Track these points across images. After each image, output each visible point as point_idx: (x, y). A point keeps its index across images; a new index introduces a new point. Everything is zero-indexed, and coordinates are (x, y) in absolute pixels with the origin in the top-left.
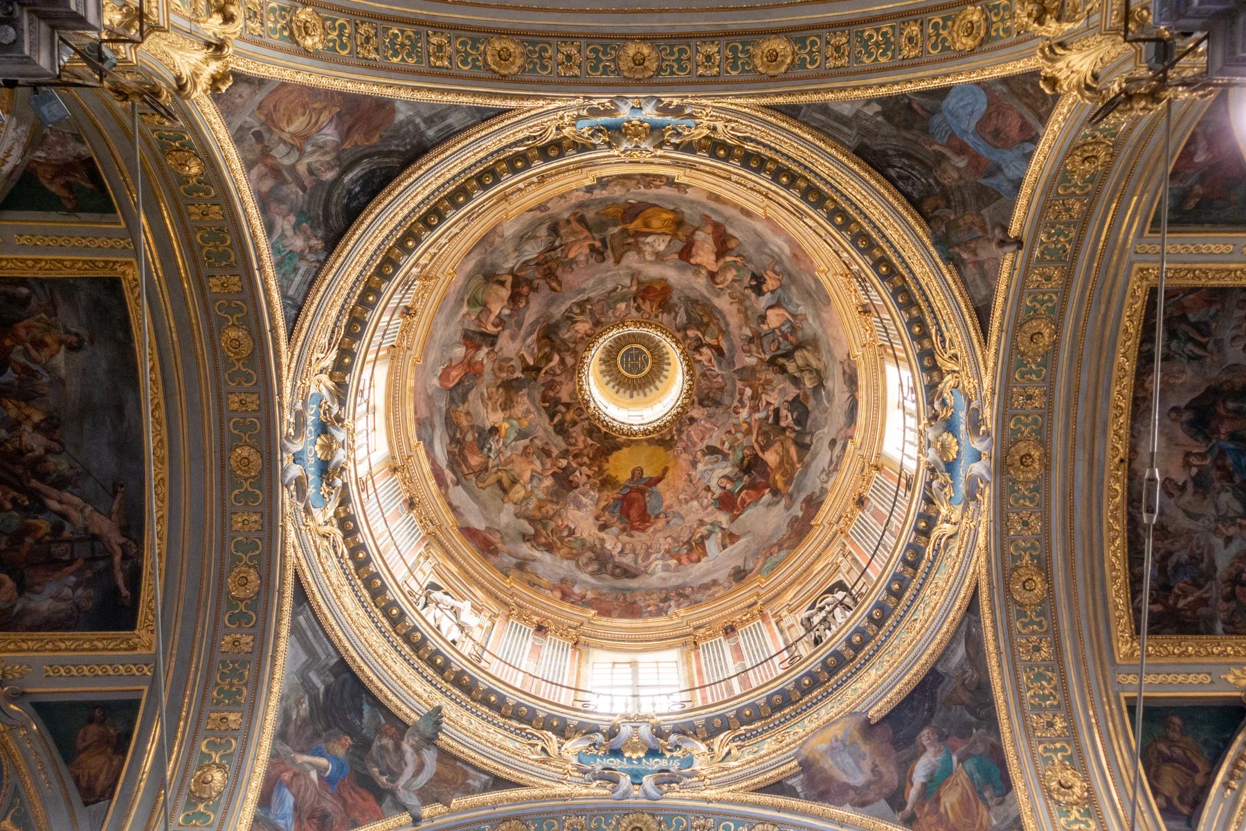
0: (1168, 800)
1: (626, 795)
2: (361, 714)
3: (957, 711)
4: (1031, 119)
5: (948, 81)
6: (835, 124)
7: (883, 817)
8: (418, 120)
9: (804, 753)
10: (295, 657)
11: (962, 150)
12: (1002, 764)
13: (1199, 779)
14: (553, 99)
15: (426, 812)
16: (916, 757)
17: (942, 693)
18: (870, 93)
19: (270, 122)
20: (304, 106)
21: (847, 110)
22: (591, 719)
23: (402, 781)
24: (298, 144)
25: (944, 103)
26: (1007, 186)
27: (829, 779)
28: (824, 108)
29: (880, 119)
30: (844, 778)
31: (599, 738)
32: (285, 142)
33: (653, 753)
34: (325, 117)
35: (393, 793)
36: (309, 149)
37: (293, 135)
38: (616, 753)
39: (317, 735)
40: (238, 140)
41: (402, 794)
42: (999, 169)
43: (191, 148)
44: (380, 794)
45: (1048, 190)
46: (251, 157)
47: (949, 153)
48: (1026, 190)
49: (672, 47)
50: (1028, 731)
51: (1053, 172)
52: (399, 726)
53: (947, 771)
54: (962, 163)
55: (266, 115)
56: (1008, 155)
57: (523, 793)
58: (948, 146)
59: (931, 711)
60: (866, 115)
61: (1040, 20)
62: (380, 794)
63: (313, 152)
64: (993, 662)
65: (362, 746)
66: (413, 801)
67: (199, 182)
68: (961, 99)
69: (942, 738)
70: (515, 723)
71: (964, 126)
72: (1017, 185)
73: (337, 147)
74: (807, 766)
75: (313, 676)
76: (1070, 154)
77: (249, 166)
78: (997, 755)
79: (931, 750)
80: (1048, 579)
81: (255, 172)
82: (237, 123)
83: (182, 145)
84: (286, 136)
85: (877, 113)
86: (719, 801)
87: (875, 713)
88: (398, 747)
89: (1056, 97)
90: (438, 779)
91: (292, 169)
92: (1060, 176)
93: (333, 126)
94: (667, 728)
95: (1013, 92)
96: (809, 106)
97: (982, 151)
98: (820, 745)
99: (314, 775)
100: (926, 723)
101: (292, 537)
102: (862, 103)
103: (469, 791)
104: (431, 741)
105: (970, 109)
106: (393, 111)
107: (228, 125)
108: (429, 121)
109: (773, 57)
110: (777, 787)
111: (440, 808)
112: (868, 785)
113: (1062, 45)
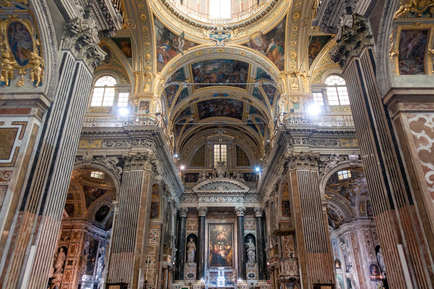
0: (311, 55)
1: (218, 46)
2: (170, 36)
3: (278, 36)
7: (262, 54)
9: (251, 38)
10: (156, 29)
12: (284, 49)
13: (318, 50)
15: (184, 52)
16: (270, 43)
17: (277, 32)
22: (212, 26)
23: (179, 47)
27: (255, 44)
30: (257, 45)
31: (213, 30)
33: (223, 33)
35: (178, 49)
38: (217, 33)
39: (163, 42)
41: (180, 49)
44: (176, 50)
50: (290, 44)
52: (176, 36)
53: (275, 47)
57: (201, 46)
59: (274, 35)
62: (176, 50)
64: (286, 30)
65: (171, 42)
66: (181, 50)
69: (275, 40)
70: (197, 28)
74: (251, 41)
75: (160, 31)
78: (283, 47)
79: (273, 42)
80: (300, 15)
86: (235, 47)
87: (264, 33)
88: (177, 41)
90: (185, 45)
94: (226, 28)
98: (253, 37)
99: (164, 50)
100: (273, 37)
101: (151, 7)
103: (191, 47)
104: (183, 38)
110: (245, 45)
111: (186, 51)
112: (261, 47)
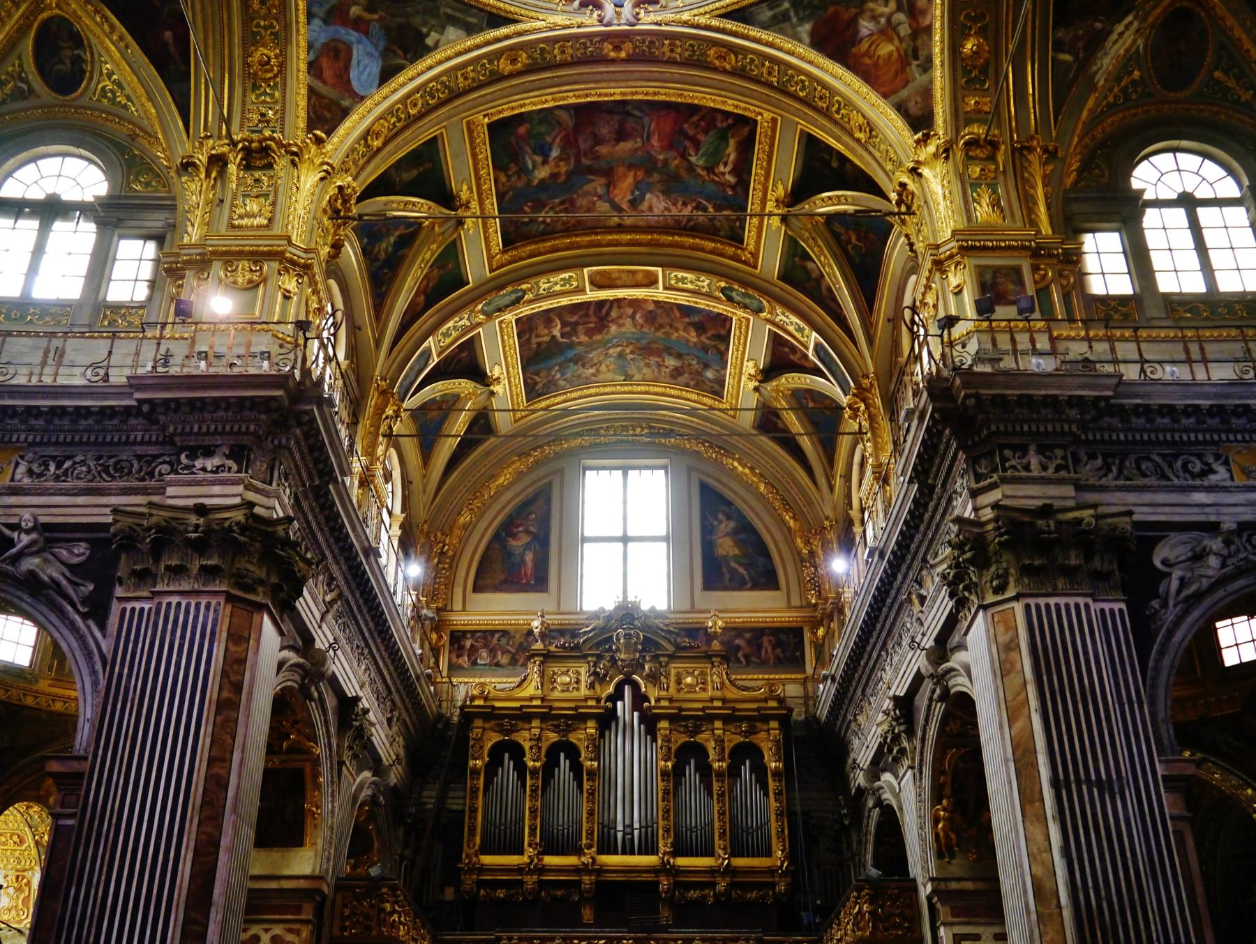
4: (318, 85)
5: (385, 90)
6: (458, 15)
8: (794, 20)
11: (358, 25)
14: (685, 24)
18: (438, 55)
19: (904, 62)
20: (876, 65)
21: (452, 32)
24: (889, 30)
25: (380, 63)
26: (315, 9)
28: (470, 30)
29: (425, 30)
32: (898, 36)
34: (864, 46)
36: (883, 20)
37: (891, 41)
40: (929, 60)
42: (326, 21)
43: (964, 68)
45: (287, 26)
46: (926, 37)
47: (367, 16)
48: (302, 18)
49: (592, 55)
51: (289, 48)
54: (355, 10)
55: (905, 71)
56: (323, 39)
58: (368, 22)
60: (436, 31)
61: (340, 188)
63: (881, 15)
67: (970, 28)
68: (369, 74)
71: (361, 47)
72: (310, 16)
73: (861, 13)
76: (282, 66)
77: (929, 30)
81: (927, 22)
82: (925, 77)
83: (970, 72)
84: (896, 42)
85: (428, 35)
89: (310, 127)
91: (899, 8)
92: (282, 39)
93: (860, 35)
95: (337, 104)
96: (480, 30)
97: (342, 30)
102: (441, 43)
105: (361, 68)
106: (813, 34)
107: (931, 82)
108: (785, 17)
109: (514, 61)
113: (322, 179)
